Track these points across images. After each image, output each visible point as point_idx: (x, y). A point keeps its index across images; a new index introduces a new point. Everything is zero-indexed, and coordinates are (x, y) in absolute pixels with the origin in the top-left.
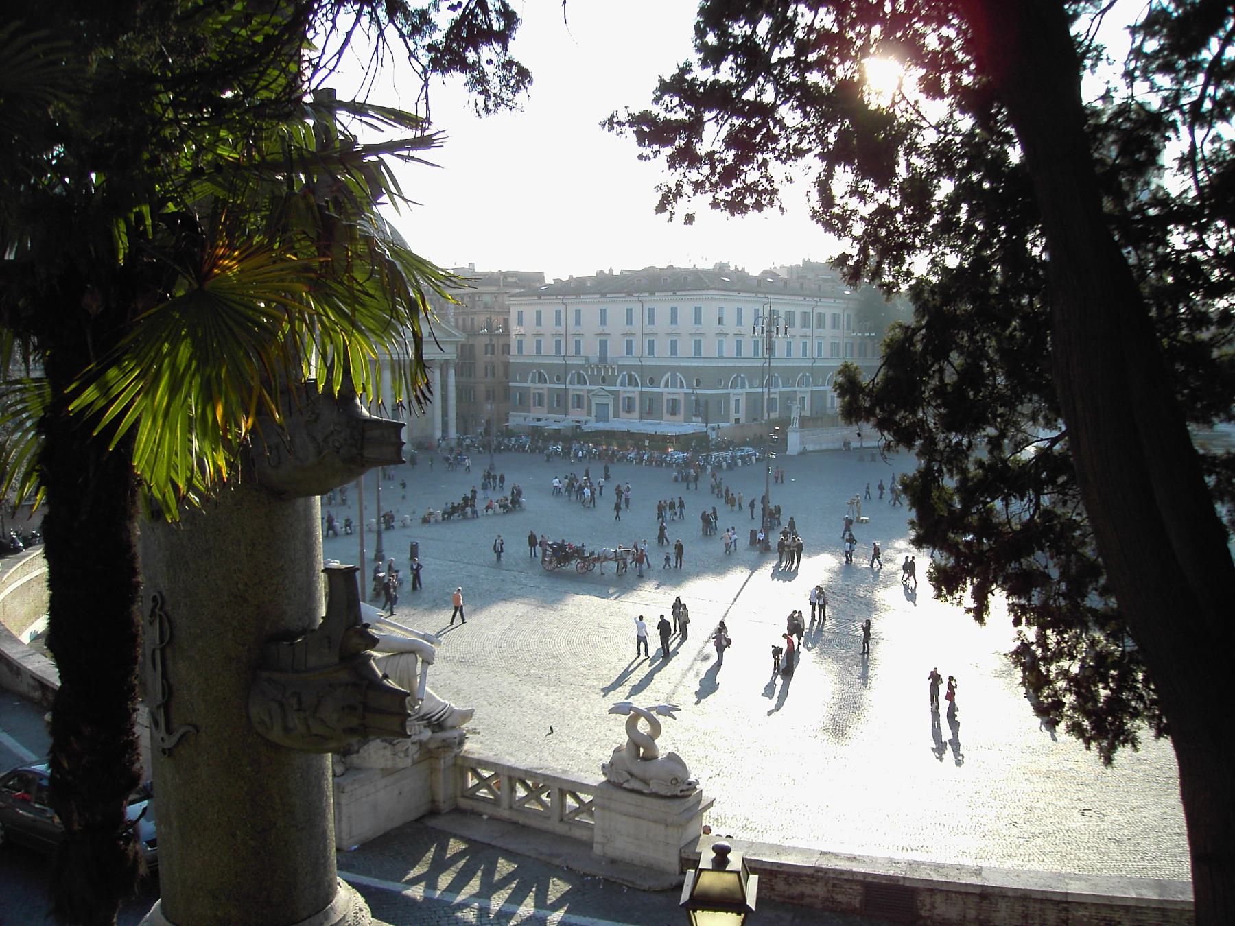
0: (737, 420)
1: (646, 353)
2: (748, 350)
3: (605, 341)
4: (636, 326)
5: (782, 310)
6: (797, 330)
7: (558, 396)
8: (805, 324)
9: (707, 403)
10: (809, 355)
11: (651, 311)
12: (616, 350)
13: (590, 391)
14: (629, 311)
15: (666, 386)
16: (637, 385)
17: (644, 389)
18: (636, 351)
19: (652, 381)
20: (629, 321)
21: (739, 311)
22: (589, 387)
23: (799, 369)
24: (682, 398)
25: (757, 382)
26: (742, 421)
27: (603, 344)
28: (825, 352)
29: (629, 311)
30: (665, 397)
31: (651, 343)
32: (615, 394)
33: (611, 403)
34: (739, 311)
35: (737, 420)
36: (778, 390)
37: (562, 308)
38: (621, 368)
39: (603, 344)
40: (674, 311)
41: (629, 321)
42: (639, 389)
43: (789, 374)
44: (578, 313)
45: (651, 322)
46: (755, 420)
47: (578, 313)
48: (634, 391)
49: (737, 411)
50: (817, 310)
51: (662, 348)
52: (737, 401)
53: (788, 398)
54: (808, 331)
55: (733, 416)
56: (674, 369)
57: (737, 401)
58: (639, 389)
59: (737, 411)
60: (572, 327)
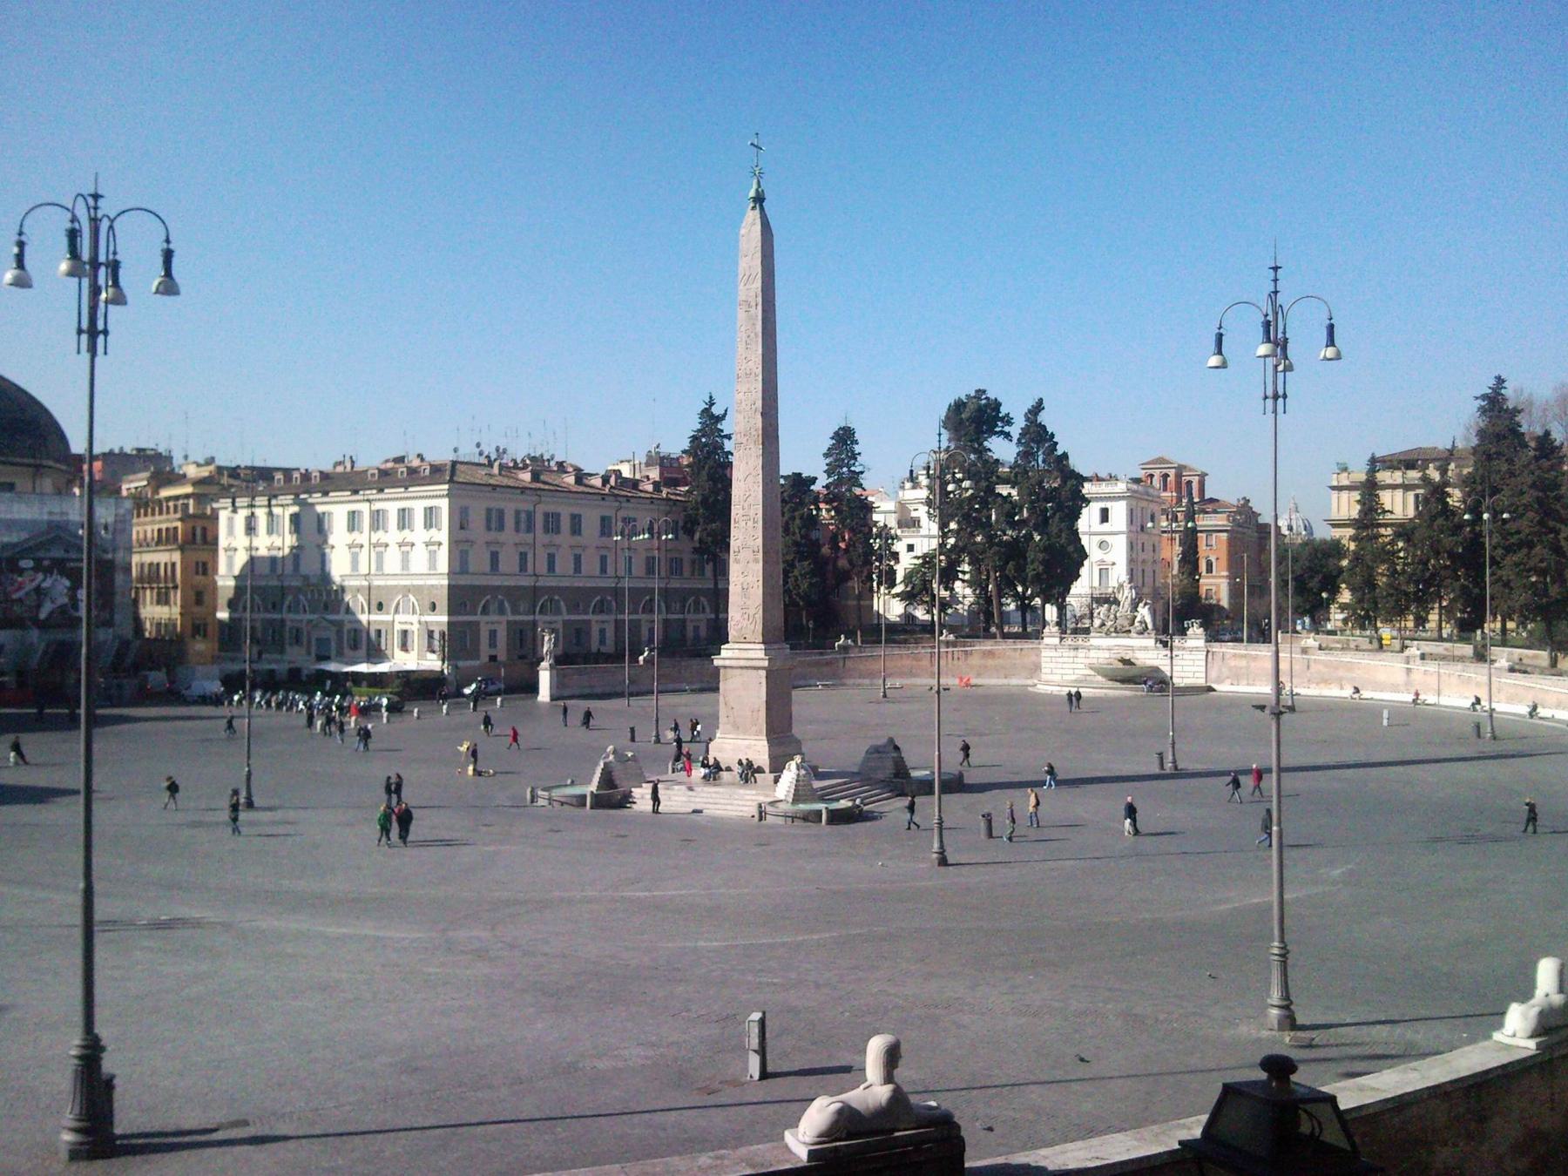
10: (610, 570)
28: (639, 568)
35: (493, 658)
46: (522, 657)
49: (493, 644)
52: (493, 634)
55: (485, 650)
57: (493, 634)
59: (493, 644)
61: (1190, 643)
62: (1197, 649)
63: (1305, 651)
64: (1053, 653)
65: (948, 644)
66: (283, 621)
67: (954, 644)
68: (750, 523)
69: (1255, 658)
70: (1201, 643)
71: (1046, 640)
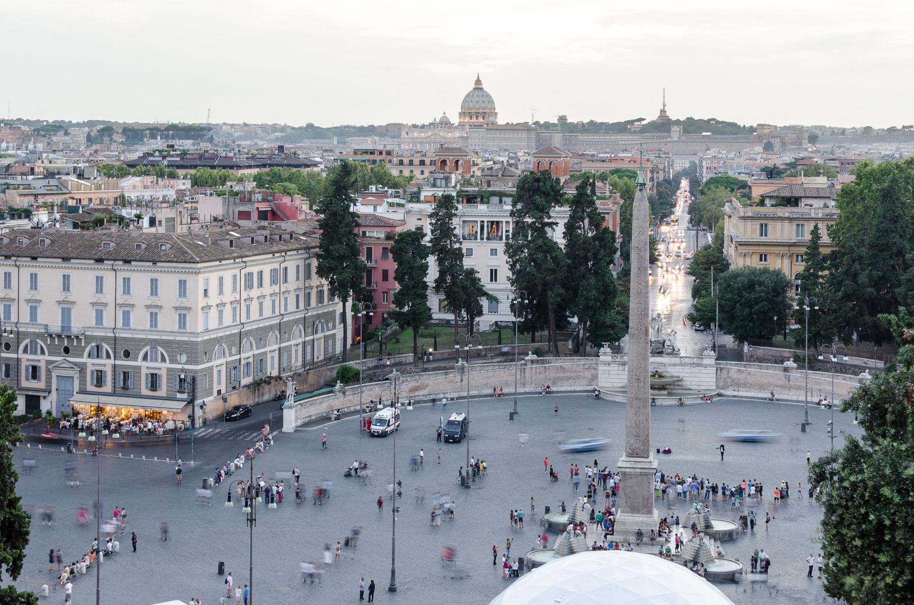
0: (219, 392)
1: (120, 324)
2: (228, 320)
3: (69, 310)
4: (108, 296)
5: (255, 270)
6: (267, 289)
7: (8, 367)
8: (274, 282)
9: (194, 379)
11: (127, 281)
12: (82, 321)
13: (49, 363)
14: (99, 280)
15: (145, 358)
16: (108, 356)
17: (118, 362)
18: (108, 322)
19: (127, 354)
20: (100, 289)
21: (221, 280)
22: (47, 357)
23: (271, 327)
24: (163, 374)
25: (234, 350)
26: (223, 392)
27: (66, 314)
28: (292, 307)
29: (99, 280)
30: (144, 372)
31: (126, 316)
32: (82, 368)
33: (76, 376)
34: (221, 280)
35: (219, 392)
36: (250, 354)
37: (13, 271)
38: (89, 339)
39: (66, 314)
40: (154, 282)
41: (100, 289)
42: (112, 361)
43: (261, 336)
44: (34, 277)
45: (127, 290)
46: (234, 388)
47: (34, 277)
48: (107, 364)
49: (219, 383)
50: (283, 265)
51: (140, 321)
53: (261, 361)
54: (276, 288)
56: (155, 343)
58: (112, 361)
59: (219, 383)
60: (26, 293)
61: (705, 362)
62: (711, 366)
63: (786, 370)
64: (607, 368)
65: (532, 362)
66: (18, 360)
67: (537, 362)
68: (641, 384)
69: (749, 374)
70: (713, 362)
71: (602, 358)
